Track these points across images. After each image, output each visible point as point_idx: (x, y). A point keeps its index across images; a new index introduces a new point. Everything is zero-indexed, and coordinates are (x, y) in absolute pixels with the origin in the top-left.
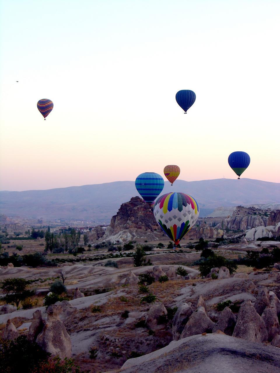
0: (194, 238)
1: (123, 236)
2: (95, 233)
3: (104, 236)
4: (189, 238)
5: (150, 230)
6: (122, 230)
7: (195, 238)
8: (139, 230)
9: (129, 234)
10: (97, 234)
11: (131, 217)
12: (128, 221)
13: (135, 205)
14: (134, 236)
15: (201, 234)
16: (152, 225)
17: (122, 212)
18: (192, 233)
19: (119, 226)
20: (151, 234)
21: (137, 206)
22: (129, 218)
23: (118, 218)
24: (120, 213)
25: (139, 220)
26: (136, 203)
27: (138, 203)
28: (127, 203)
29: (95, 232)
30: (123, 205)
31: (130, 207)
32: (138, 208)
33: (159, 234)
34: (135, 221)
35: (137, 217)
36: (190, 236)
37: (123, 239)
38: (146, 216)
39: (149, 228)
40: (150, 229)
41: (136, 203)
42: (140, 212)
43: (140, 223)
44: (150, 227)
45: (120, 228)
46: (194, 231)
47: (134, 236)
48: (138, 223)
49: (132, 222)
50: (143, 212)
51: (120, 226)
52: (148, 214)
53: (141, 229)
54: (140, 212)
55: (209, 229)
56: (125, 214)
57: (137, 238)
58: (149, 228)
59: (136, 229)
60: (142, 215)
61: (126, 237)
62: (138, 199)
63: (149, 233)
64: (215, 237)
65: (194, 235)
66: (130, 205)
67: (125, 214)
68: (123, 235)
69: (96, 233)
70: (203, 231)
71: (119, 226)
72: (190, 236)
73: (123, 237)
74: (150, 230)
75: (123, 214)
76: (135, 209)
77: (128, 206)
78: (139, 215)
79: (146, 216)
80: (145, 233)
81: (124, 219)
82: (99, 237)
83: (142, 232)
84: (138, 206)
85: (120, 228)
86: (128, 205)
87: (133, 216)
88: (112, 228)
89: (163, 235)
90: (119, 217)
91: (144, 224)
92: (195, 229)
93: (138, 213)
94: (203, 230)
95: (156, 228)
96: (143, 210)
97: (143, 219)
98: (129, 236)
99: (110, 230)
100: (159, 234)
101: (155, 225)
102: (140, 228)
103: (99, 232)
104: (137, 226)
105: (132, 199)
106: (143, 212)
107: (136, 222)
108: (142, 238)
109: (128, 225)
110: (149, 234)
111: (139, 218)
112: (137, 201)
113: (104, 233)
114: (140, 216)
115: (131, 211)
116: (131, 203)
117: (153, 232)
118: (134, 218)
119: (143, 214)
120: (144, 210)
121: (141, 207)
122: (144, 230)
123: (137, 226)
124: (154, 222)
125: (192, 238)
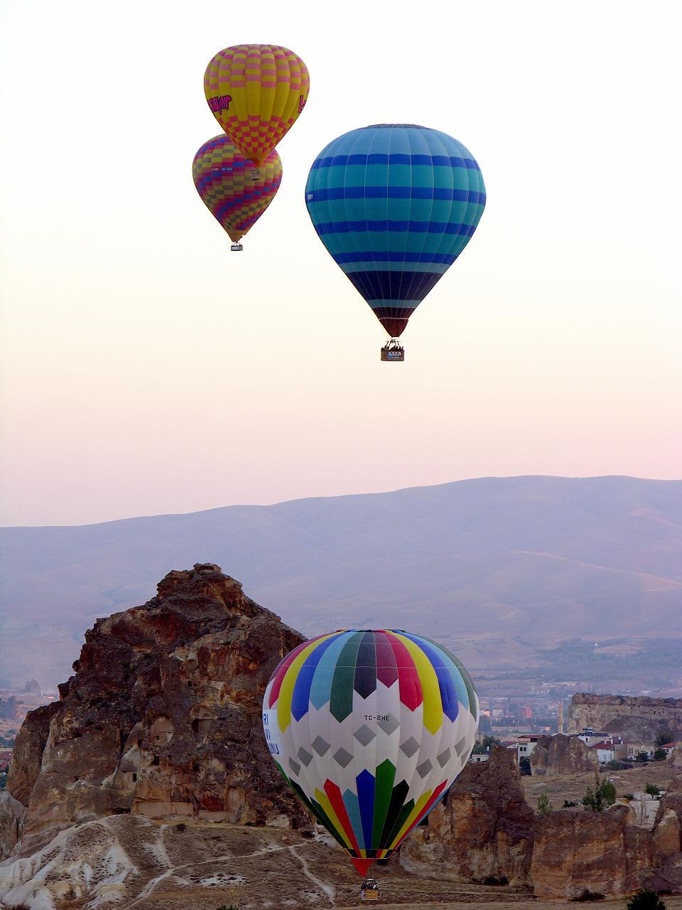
0: (610, 885)
1: (72, 868)
4: (569, 891)
5: (284, 822)
6: (80, 816)
7: (617, 885)
8: (212, 820)
9: (117, 855)
11: (150, 723)
12: (132, 755)
13: (186, 632)
14: (149, 867)
15: (665, 858)
17: (97, 679)
18: (594, 852)
19: (63, 792)
20: (288, 852)
21: (198, 636)
22: (139, 725)
23: (60, 724)
24: (83, 691)
25: (205, 741)
26: (196, 615)
27: (212, 613)
28: (132, 612)
30: (105, 629)
31: (151, 643)
32: (203, 653)
34: (175, 747)
35: (196, 724)
37: (62, 889)
40: (284, 811)
41: (196, 615)
42: (220, 686)
43: (216, 764)
45: (71, 807)
46: (611, 835)
47: (149, 867)
48: (196, 768)
49: (155, 762)
51: (71, 787)
53: (219, 815)
56: (112, 696)
57: (168, 886)
58: (278, 802)
60: (234, 706)
61: (89, 873)
62: (215, 589)
63: (275, 848)
65: (606, 864)
66: (149, 630)
67: (112, 696)
68: (68, 859)
71: (63, 792)
72: (580, 872)
73: (67, 876)
74: (284, 822)
75: (102, 694)
76: (179, 663)
77: (140, 640)
78: (208, 703)
80: (244, 847)
81: (98, 738)
83: (218, 839)
84: (207, 640)
85: (71, 807)
86: (138, 632)
88: (14, 801)
90: (70, 721)
91: (239, 777)
92: (618, 813)
93: (203, 690)
96: (238, 672)
97: (239, 736)
98: (113, 868)
102: (216, 804)
104: (190, 786)
105: (170, 584)
107: (183, 761)
108: (207, 882)
109: (127, 777)
110: (271, 855)
111: (206, 725)
112: (202, 603)
114: (217, 710)
115: (154, 676)
116: (158, 611)
117: (308, 835)
118: (171, 728)
119: (238, 700)
120: (247, 671)
121: (227, 648)
123: (190, 786)
125: (592, 888)
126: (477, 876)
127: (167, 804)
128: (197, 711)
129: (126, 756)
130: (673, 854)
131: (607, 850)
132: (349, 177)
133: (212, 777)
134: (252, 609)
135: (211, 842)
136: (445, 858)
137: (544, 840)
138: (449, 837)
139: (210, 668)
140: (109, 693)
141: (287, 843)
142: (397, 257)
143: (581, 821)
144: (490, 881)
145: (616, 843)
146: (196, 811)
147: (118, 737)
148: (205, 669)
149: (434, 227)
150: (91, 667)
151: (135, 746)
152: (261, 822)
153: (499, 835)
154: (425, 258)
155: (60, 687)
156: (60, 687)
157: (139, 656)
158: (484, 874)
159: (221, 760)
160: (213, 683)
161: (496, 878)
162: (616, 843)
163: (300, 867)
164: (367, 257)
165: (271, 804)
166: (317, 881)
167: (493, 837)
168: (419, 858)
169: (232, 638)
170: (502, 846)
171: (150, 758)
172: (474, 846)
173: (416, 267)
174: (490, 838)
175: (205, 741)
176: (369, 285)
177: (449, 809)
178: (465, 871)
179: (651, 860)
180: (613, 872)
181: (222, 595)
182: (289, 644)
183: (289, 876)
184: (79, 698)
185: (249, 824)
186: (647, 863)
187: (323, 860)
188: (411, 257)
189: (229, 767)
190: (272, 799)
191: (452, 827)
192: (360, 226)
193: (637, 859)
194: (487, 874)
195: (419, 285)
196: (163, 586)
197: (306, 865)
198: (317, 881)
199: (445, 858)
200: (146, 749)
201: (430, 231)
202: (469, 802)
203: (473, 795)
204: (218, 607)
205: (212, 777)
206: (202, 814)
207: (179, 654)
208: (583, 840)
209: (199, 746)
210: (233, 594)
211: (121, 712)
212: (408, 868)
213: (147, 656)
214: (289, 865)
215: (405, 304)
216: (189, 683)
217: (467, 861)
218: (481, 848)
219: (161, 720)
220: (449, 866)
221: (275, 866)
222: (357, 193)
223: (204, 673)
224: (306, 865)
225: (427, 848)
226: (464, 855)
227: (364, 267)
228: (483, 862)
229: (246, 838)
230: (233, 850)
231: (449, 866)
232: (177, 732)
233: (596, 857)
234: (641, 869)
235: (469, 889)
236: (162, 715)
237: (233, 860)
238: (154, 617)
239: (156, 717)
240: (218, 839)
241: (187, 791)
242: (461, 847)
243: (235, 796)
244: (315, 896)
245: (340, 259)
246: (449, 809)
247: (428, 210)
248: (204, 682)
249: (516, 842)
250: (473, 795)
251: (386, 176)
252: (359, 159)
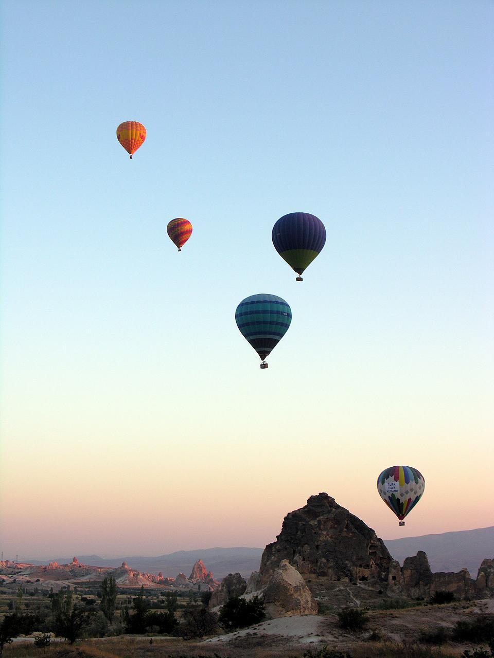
2: (222, 590)
5: (347, 580)
8: (323, 579)
10: (229, 592)
11: (302, 547)
13: (315, 515)
16: (354, 565)
20: (346, 589)
22: (299, 548)
25: (320, 552)
26: (320, 510)
29: (223, 586)
30: (290, 516)
32: (319, 522)
33: (370, 588)
35: (317, 547)
38: (340, 542)
39: (345, 573)
41: (320, 510)
42: (325, 533)
44: (349, 570)
48: (317, 562)
49: (304, 560)
50: (331, 532)
53: (326, 578)
54: (325, 533)
56: (292, 538)
58: (345, 573)
60: (329, 539)
62: (326, 501)
63: (342, 588)
69: (225, 590)
70: (487, 581)
74: (347, 580)
78: (321, 539)
79: (340, 542)
80: (331, 588)
81: (285, 552)
83: (322, 585)
84: (321, 517)
87: (308, 545)
89: (380, 592)
92: (462, 573)
95: (366, 572)
97: (331, 550)
99: (258, 582)
100: (370, 588)
101: (361, 566)
102: (324, 574)
103: (234, 587)
104: (315, 568)
105: (312, 500)
106: (331, 532)
110: (340, 590)
111: (320, 547)
112: (321, 506)
117: (355, 584)
118: (309, 548)
121: (328, 520)
122: (331, 579)
124: (359, 559)
126: (413, 597)
127: (308, 574)
128: (318, 542)
129: (295, 558)
130: (483, 588)
131: (458, 586)
132: (250, 308)
133: (322, 565)
134: (338, 507)
135: (319, 586)
136: (402, 591)
137: (434, 583)
138: (403, 583)
139: (322, 527)
140: (291, 537)
141: (347, 586)
142: (265, 333)
143: (448, 576)
144: (418, 599)
146: (318, 576)
147: (292, 552)
148: (320, 527)
149: (277, 323)
150: (286, 529)
151: (298, 555)
152: (339, 580)
153: (421, 582)
154: (275, 334)
155: (277, 536)
156: (277, 536)
157: (301, 525)
158: (416, 597)
159: (325, 558)
160: (323, 532)
161: (420, 598)
162: (461, 584)
163: (349, 594)
164: (256, 333)
165: (342, 573)
166: (354, 599)
167: (419, 583)
168: (393, 591)
169: (329, 517)
171: (302, 558)
172: (412, 587)
173: (271, 337)
174: (417, 583)
175: (320, 552)
176: (256, 344)
177: (403, 573)
178: (409, 596)
179: (475, 591)
181: (328, 503)
182: (328, 511)
183: (344, 597)
184: (282, 540)
185: (335, 580)
186: (473, 592)
187: (358, 592)
188: (270, 333)
189: (328, 561)
190: (342, 572)
191: (404, 579)
192: (253, 323)
193: (469, 590)
194: (417, 596)
195: (273, 343)
196: (309, 501)
197: (351, 593)
198: (354, 599)
199: (402, 591)
200: (301, 555)
201: (247, 312)
202: (410, 571)
203: (411, 568)
204: (327, 507)
205: (322, 565)
206: (319, 577)
207: (312, 523)
209: (318, 553)
210: (331, 501)
211: (294, 544)
212: (389, 595)
213: (304, 525)
214: (345, 593)
215: (266, 349)
216: (315, 532)
217: (409, 592)
218: (415, 586)
219: (306, 545)
220: (403, 594)
221: (340, 594)
222: (252, 313)
223: (320, 529)
224: (351, 593)
225: (395, 588)
226: (408, 590)
227: (255, 337)
228: (415, 592)
229: (332, 585)
230: (326, 589)
231: (403, 594)
232: (311, 549)
233: (454, 589)
234: (471, 593)
235: (411, 602)
236: (306, 544)
237: (326, 592)
238: (306, 511)
239: (304, 544)
240: (322, 585)
241: (314, 569)
243: (330, 571)
244: (352, 604)
245: (245, 336)
246: (403, 573)
247: (275, 318)
248: (320, 532)
249: (426, 585)
250: (411, 568)
251: (261, 307)
252: (252, 303)
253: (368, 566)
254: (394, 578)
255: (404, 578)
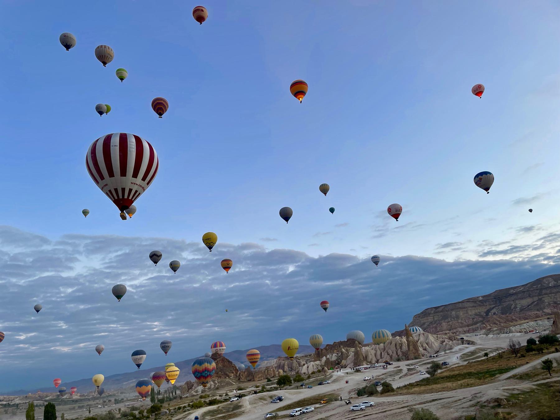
3: (193, 387)
14: (215, 384)
16: (229, 373)
18: (260, 375)
21: (216, 360)
27: (218, 357)
32: (217, 361)
36: (259, 378)
43: (220, 372)
46: (261, 373)
47: (216, 384)
50: (222, 364)
52: (225, 365)
55: (272, 371)
59: (217, 378)
60: (221, 366)
64: (277, 375)
65: (261, 377)
72: (259, 378)
82: (189, 389)
84: (218, 360)
94: (268, 371)
106: (222, 364)
112: (216, 356)
113: (193, 385)
145: (262, 374)
168: (242, 379)
170: (250, 377)
178: (247, 380)
180: (262, 377)
189: (221, 373)
208: (259, 374)
226: (246, 378)
242: (246, 377)
253: (233, 373)
254: (242, 375)
255: (245, 375)
